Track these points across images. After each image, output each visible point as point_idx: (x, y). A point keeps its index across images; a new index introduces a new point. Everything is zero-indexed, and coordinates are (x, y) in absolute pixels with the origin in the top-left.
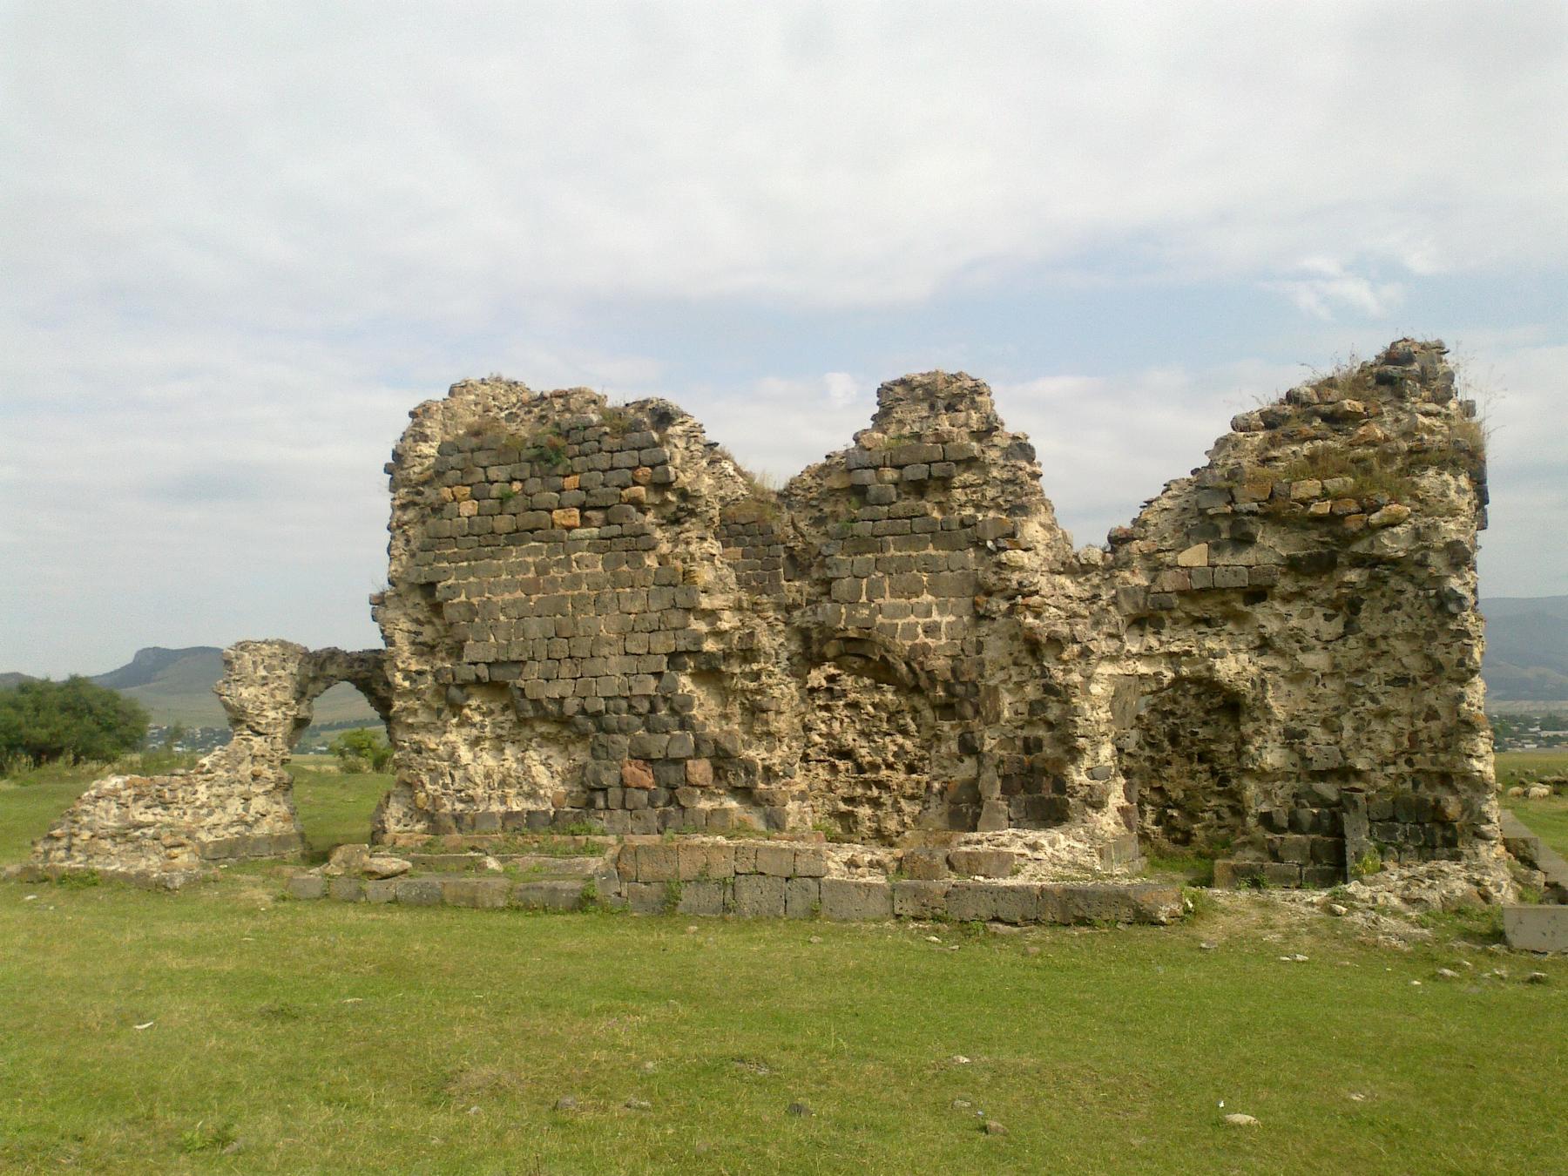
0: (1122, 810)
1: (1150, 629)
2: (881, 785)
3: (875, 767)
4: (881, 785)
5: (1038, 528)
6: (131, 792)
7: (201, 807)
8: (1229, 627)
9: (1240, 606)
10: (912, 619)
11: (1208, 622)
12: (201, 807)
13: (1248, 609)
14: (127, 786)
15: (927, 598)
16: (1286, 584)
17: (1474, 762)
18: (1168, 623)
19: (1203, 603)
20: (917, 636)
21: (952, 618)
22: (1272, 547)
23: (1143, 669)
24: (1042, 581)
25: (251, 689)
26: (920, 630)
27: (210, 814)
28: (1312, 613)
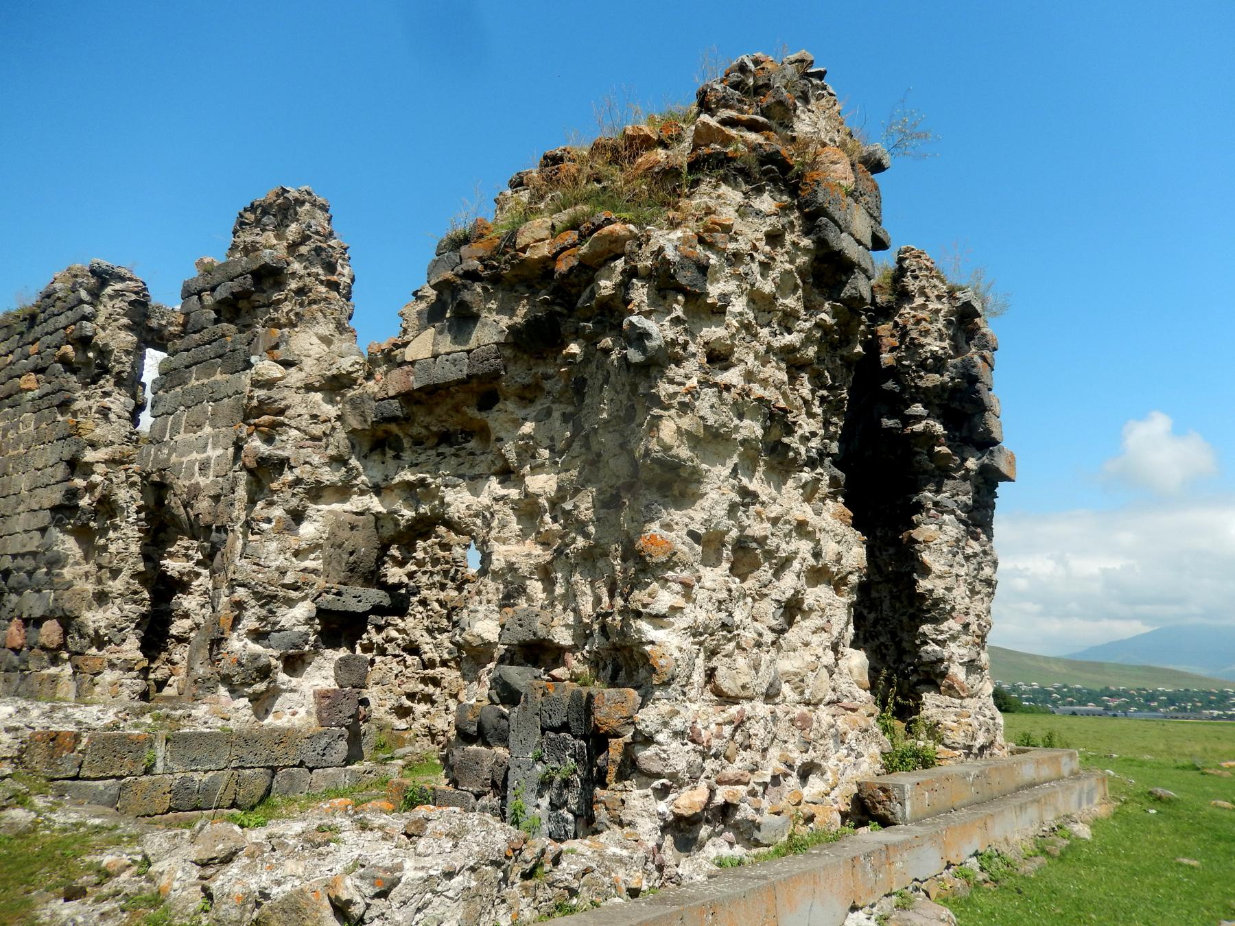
0: (322, 696)
1: (390, 453)
2: (436, 682)
3: (431, 664)
4: (436, 682)
5: (315, 340)
8: (472, 444)
9: (472, 412)
10: (195, 455)
11: (445, 438)
13: (484, 414)
15: (207, 429)
16: (518, 375)
17: (643, 625)
18: (406, 443)
19: (438, 411)
20: (193, 475)
21: (220, 451)
22: (493, 326)
23: (376, 504)
24: (294, 398)
26: (197, 468)
28: (549, 413)
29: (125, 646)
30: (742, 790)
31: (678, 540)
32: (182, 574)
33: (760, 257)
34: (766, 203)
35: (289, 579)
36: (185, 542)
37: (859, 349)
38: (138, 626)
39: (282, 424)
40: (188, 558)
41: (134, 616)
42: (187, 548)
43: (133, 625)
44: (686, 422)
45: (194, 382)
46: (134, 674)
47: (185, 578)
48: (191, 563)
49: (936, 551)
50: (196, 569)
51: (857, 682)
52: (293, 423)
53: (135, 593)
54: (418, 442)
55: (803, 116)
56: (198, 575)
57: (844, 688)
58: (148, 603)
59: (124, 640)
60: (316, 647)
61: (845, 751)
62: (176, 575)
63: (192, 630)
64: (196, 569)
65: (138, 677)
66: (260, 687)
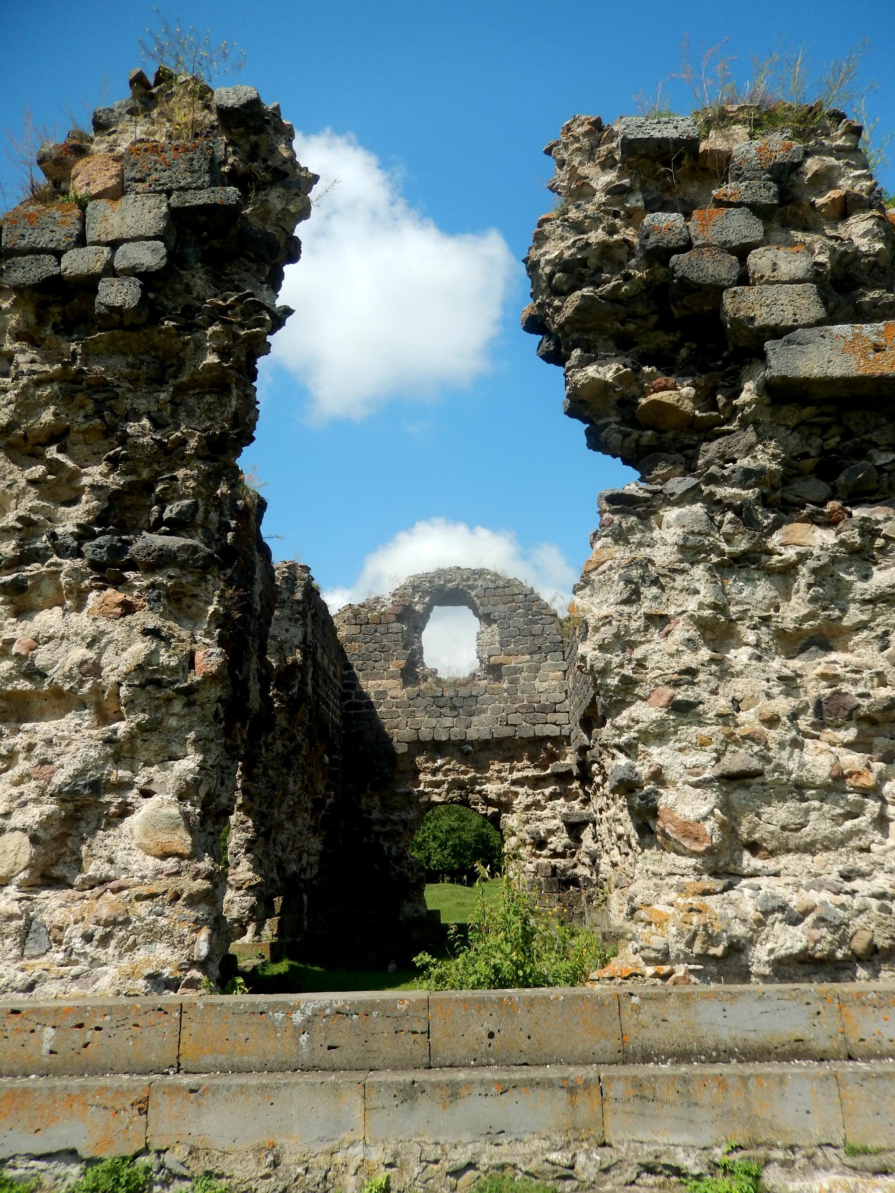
29: (239, 869)
32: (499, 795)
36: (496, 766)
37: (212, 359)
38: (248, 851)
40: (502, 780)
41: (242, 842)
42: (500, 771)
43: (243, 851)
46: (242, 892)
47: (503, 799)
48: (506, 784)
49: (603, 584)
50: (513, 788)
51: (140, 846)
53: (243, 823)
56: (516, 794)
57: (120, 856)
58: (251, 830)
59: (238, 864)
61: (60, 956)
62: (494, 797)
63: (519, 847)
64: (513, 788)
65: (247, 895)
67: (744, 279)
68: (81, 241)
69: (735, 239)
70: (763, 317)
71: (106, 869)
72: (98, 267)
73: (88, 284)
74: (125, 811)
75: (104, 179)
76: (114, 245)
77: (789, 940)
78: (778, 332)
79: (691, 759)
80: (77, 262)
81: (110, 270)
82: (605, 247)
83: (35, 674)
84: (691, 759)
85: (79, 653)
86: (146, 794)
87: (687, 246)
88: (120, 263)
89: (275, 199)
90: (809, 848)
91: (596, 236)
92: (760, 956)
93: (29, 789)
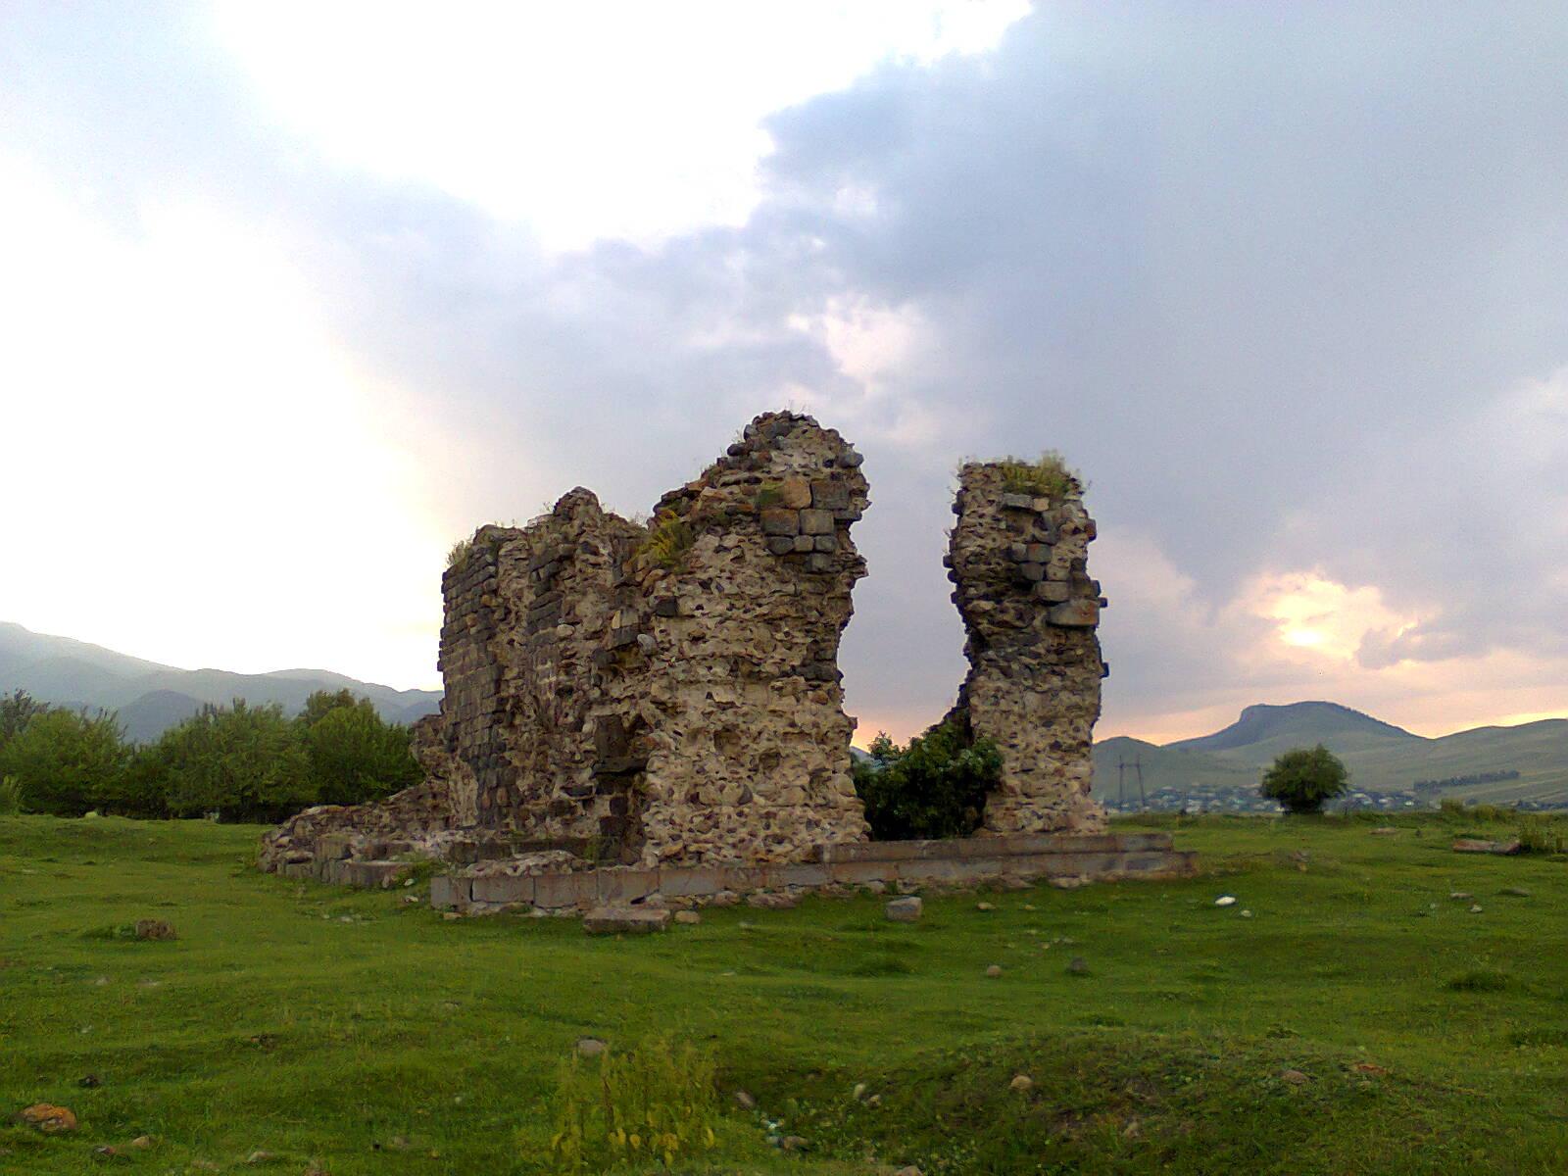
0: (604, 821)
6: (325, 816)
7: (385, 827)
12: (385, 827)
14: (321, 813)
18: (625, 673)
25: (435, 749)
27: (393, 830)
30: (710, 846)
31: (666, 738)
33: (727, 574)
34: (730, 541)
35: (577, 757)
39: (573, 664)
44: (664, 682)
45: (541, 632)
52: (578, 662)
54: (631, 672)
55: (778, 460)
57: (831, 797)
60: (598, 792)
66: (568, 816)
67: (1045, 578)
68: (801, 533)
69: (1042, 560)
70: (1050, 597)
71: (822, 802)
72: (810, 547)
73: (807, 553)
74: (829, 779)
75: (806, 500)
76: (814, 535)
77: (1038, 824)
78: (1054, 603)
79: (1014, 764)
80: (802, 543)
81: (815, 551)
82: (992, 549)
83: (793, 725)
84: (1014, 764)
85: (809, 718)
86: (834, 772)
87: (1027, 562)
88: (819, 547)
89: (859, 501)
90: (1043, 796)
91: (990, 544)
92: (1029, 829)
93: (800, 770)
